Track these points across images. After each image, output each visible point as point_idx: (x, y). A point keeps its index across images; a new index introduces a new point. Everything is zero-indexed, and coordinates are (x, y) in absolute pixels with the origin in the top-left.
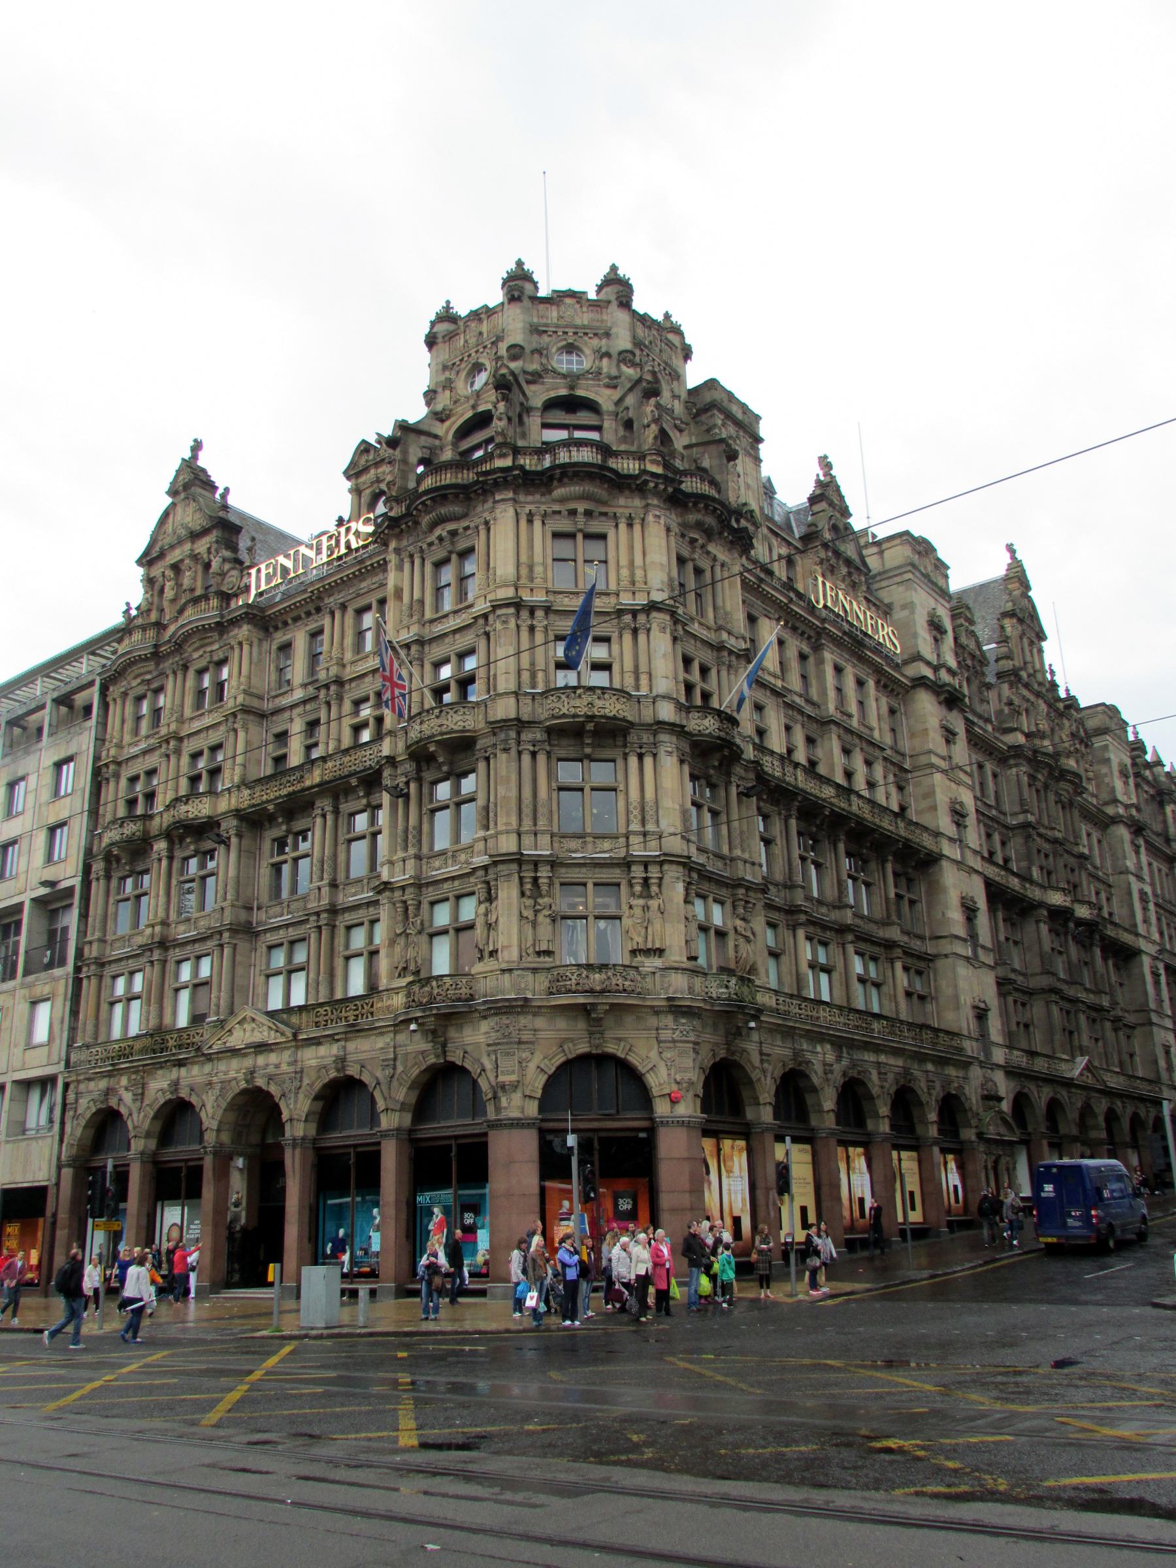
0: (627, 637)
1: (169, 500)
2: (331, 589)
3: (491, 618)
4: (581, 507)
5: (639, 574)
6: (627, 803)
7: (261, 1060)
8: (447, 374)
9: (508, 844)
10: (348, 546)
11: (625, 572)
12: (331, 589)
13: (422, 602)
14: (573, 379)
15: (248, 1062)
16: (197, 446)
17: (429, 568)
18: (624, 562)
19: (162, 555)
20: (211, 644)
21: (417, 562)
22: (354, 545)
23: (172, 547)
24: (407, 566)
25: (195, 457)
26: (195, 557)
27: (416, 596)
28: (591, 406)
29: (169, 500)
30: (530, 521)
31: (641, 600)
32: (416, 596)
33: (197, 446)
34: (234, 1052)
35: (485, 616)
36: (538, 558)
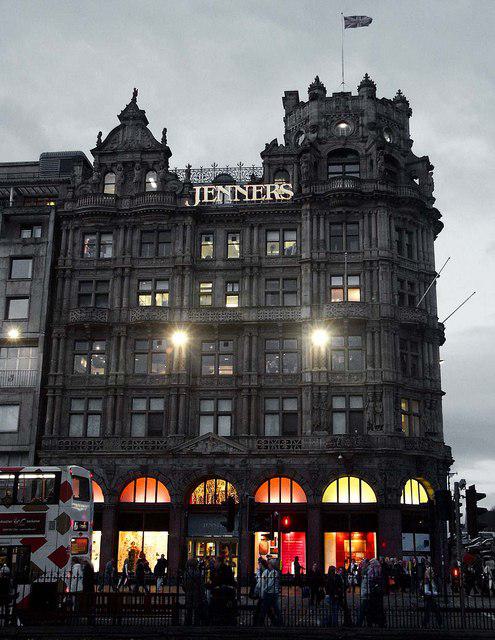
1: (118, 123)
2: (252, 215)
3: (375, 264)
4: (409, 218)
6: (423, 363)
7: (218, 462)
9: (388, 376)
10: (273, 195)
12: (252, 215)
13: (325, 241)
15: (209, 462)
16: (135, 93)
19: (114, 153)
20: (162, 220)
21: (322, 220)
22: (277, 197)
23: (126, 152)
25: (134, 100)
27: (322, 238)
29: (118, 123)
32: (322, 238)
33: (135, 93)
34: (200, 455)
35: (371, 262)
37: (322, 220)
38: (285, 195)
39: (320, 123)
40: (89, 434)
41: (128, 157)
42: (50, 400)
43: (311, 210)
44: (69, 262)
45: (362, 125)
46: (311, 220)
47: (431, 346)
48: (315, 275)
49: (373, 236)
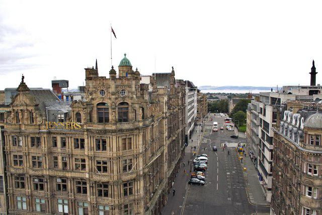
0: (135, 159)
3: (111, 159)
5: (137, 147)
8: (94, 89)
11: (135, 146)
13: (93, 147)
14: (124, 98)
16: (23, 77)
17: (95, 140)
18: (135, 144)
21: (92, 138)
24: (89, 138)
26: (27, 110)
27: (92, 146)
28: (127, 104)
30: (119, 137)
31: (138, 151)
32: (92, 146)
33: (23, 77)
36: (120, 146)
37: (92, 138)
38: (78, 127)
39: (93, 91)
40: (24, 209)
41: (22, 108)
42: (9, 198)
43: (87, 135)
44: (8, 149)
45: (109, 93)
46: (88, 138)
47: (138, 182)
48: (90, 161)
49: (111, 147)
